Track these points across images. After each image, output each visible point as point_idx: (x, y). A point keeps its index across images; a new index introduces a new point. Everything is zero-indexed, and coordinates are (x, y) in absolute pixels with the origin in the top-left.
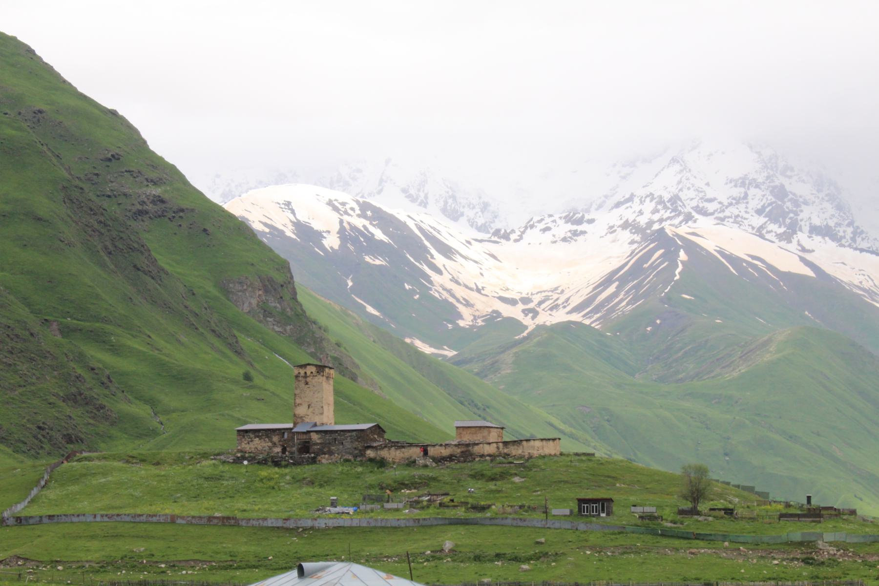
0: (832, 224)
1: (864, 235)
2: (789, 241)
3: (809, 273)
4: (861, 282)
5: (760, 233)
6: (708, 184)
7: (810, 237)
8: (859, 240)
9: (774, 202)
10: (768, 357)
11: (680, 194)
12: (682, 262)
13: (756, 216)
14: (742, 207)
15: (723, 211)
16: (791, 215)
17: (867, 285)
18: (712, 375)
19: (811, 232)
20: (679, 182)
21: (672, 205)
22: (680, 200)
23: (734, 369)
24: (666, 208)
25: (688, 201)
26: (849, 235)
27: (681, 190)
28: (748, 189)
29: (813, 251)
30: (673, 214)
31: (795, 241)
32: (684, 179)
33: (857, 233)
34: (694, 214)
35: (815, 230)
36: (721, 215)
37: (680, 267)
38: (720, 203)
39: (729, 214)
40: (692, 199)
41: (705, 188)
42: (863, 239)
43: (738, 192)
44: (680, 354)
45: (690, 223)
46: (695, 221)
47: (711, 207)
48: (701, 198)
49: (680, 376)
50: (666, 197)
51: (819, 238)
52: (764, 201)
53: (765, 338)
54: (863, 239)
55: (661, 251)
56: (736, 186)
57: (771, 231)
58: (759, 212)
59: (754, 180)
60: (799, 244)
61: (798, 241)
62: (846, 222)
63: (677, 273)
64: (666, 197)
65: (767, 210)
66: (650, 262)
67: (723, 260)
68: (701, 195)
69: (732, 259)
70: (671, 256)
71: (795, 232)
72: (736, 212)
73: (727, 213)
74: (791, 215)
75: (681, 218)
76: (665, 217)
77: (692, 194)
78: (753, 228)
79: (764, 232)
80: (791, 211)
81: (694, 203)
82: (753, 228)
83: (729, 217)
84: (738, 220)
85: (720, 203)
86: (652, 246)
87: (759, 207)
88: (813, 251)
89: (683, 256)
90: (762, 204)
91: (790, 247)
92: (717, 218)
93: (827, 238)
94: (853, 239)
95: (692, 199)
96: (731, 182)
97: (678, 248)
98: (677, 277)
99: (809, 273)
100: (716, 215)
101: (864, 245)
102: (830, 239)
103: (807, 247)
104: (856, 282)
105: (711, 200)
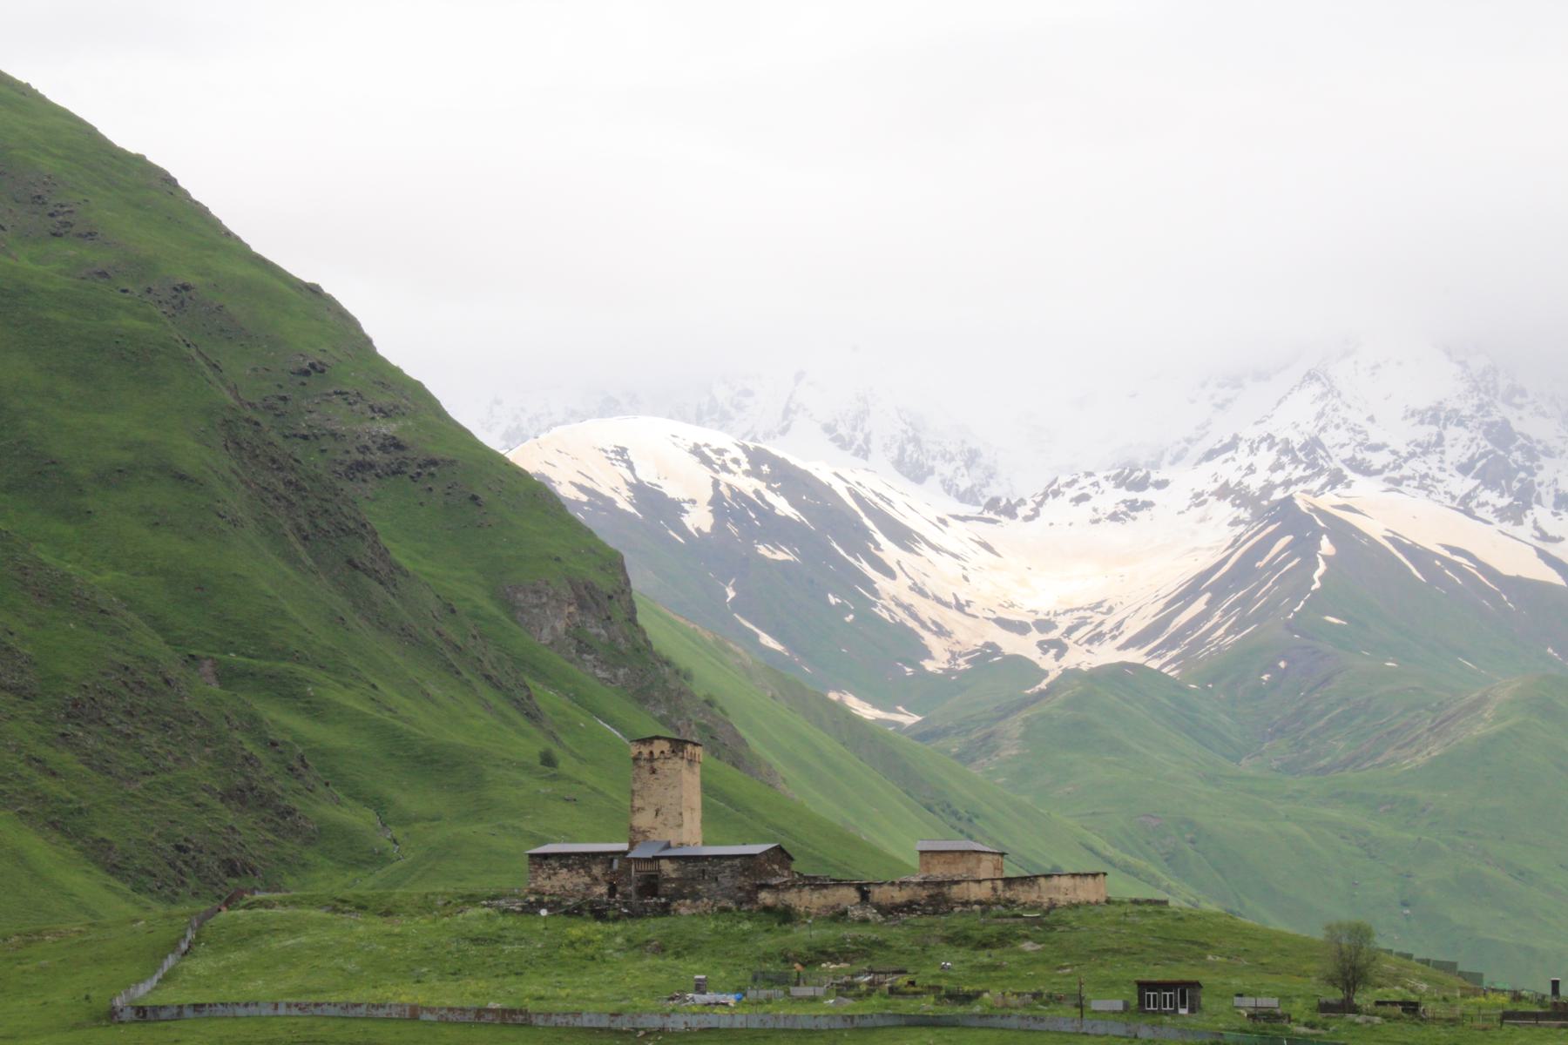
5: (1465, 506)
6: (1371, 419)
7: (1555, 514)
10: (1479, 730)
11: (1322, 436)
12: (1324, 557)
13: (1459, 477)
14: (1433, 459)
15: (1400, 467)
18: (1380, 760)
19: (1557, 505)
20: (1321, 415)
21: (1307, 455)
22: (1322, 447)
23: (1419, 751)
24: (1295, 461)
25: (1336, 450)
27: (1323, 429)
28: (1445, 427)
29: (1561, 539)
30: (1309, 472)
31: (1528, 521)
34: (1347, 471)
36: (1396, 474)
38: (1394, 452)
40: (1342, 446)
41: (1367, 426)
43: (1426, 432)
44: (1321, 723)
45: (1340, 489)
46: (1349, 485)
47: (1377, 459)
48: (1360, 444)
49: (1323, 762)
50: (1297, 441)
52: (1474, 448)
53: (1476, 695)
55: (1287, 539)
56: (1422, 422)
57: (1485, 504)
58: (1464, 469)
59: (1456, 411)
60: (1536, 527)
61: (1535, 522)
63: (1316, 576)
64: (1297, 441)
65: (1479, 465)
66: (1268, 558)
68: (1359, 438)
69: (1418, 554)
70: (1305, 547)
72: (1423, 469)
73: (1406, 470)
74: (1522, 475)
75: (1323, 479)
76: (1294, 477)
77: (1343, 435)
78: (1453, 498)
79: (1473, 504)
80: (1522, 468)
81: (1347, 453)
82: (1453, 498)
83: (1409, 478)
84: (1425, 484)
85: (1394, 452)
86: (1271, 528)
87: (1464, 460)
88: (1561, 539)
89: (1326, 546)
90: (1469, 454)
92: (1388, 480)
95: (1342, 446)
96: (1413, 415)
97: (1319, 532)
98: (1317, 585)
100: (1387, 474)
103: (1550, 533)
105: (1376, 448)
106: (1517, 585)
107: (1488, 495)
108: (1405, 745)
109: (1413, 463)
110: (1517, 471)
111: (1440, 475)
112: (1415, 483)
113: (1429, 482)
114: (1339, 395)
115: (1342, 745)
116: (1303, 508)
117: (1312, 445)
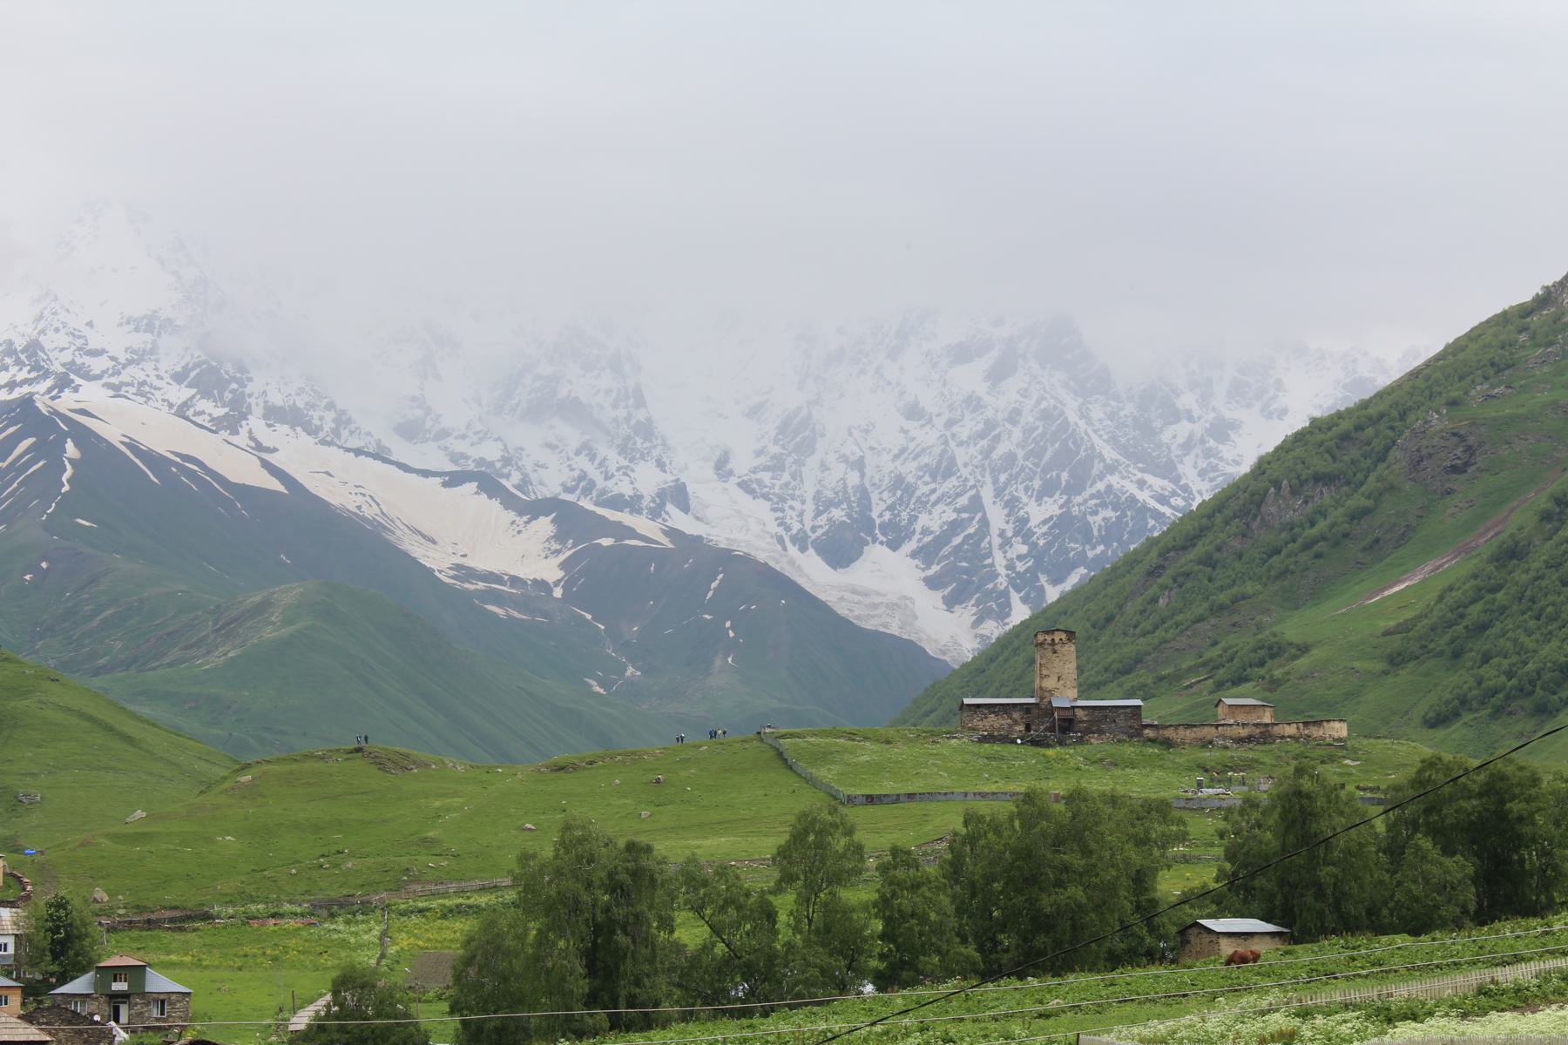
0: (301, 404)
1: (352, 427)
2: (235, 432)
3: (281, 488)
4: (359, 507)
5: (182, 412)
6: (90, 324)
7: (269, 426)
8: (345, 433)
9: (204, 362)
10: (269, 633)
11: (42, 338)
12: (70, 461)
13: (175, 386)
14: (149, 366)
15: (119, 373)
16: (234, 386)
17: (369, 512)
18: (167, 660)
19: (265, 417)
20: (40, 318)
21: (29, 358)
22: (43, 350)
23: (208, 653)
24: (18, 362)
25: (56, 353)
26: (329, 425)
27: (43, 332)
28: (159, 335)
29: (275, 450)
30: (33, 374)
31: (244, 431)
32: (47, 313)
33: (342, 420)
34: (72, 376)
35: (274, 415)
36: (115, 380)
37: (69, 472)
38: (112, 358)
39: (128, 379)
40: (63, 349)
41: (86, 331)
42: (352, 433)
43: (141, 340)
44: (95, 623)
45: (67, 393)
46: (76, 390)
47: (97, 365)
48: (79, 349)
49: (102, 661)
50: (20, 343)
51: (284, 429)
52: (187, 358)
53: (257, 599)
54: (352, 433)
55: (31, 440)
56: (137, 330)
57: (203, 413)
58: (179, 378)
59: (170, 321)
60: (252, 438)
61: (250, 432)
62: (325, 402)
63: (64, 479)
64: (20, 343)
65: (192, 375)
66: (10, 459)
67: (137, 461)
68: (79, 342)
69: (150, 457)
70: (49, 449)
71: (244, 416)
72: (141, 376)
73: (125, 377)
74: (234, 386)
75: (49, 382)
76: (19, 379)
77: (63, 339)
78: (171, 406)
79: (190, 413)
80: (234, 379)
81: (66, 357)
82: (171, 406)
83: (128, 384)
84: (144, 391)
85: (112, 358)
86: (11, 430)
87: (178, 369)
88: (275, 450)
89: (70, 445)
90: (183, 363)
91: (234, 439)
92: (108, 386)
93: (299, 429)
94: (336, 432)
95: (63, 349)
96: (128, 322)
97: (63, 437)
98: (66, 488)
99: (281, 488)
100: (106, 379)
101: (355, 443)
102: (305, 430)
103: (266, 444)
104: (352, 507)
105: (95, 353)
106: (245, 492)
107: (204, 405)
108: (192, 646)
109: (131, 370)
110: (229, 382)
111: (157, 383)
112: (134, 390)
113: (147, 389)
114: (56, 299)
115: (119, 645)
116: (44, 411)
117: (33, 348)
